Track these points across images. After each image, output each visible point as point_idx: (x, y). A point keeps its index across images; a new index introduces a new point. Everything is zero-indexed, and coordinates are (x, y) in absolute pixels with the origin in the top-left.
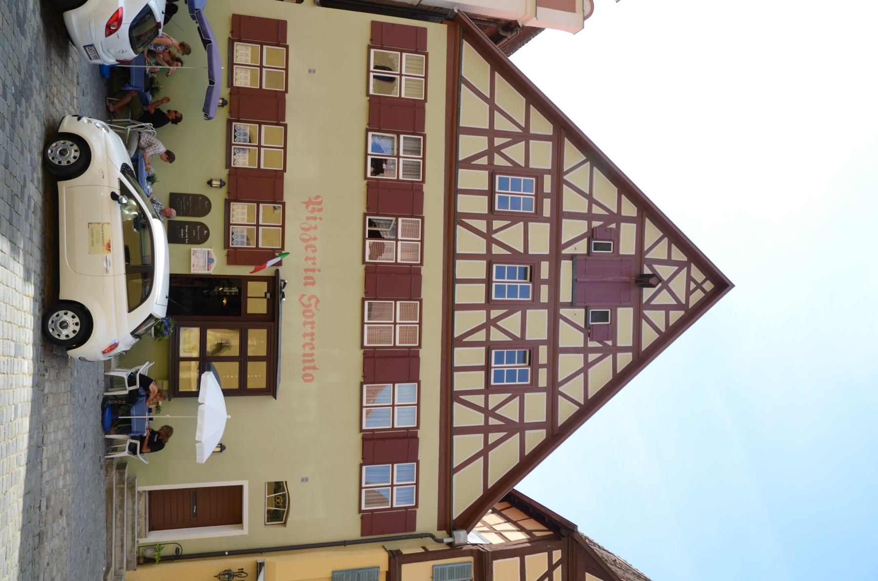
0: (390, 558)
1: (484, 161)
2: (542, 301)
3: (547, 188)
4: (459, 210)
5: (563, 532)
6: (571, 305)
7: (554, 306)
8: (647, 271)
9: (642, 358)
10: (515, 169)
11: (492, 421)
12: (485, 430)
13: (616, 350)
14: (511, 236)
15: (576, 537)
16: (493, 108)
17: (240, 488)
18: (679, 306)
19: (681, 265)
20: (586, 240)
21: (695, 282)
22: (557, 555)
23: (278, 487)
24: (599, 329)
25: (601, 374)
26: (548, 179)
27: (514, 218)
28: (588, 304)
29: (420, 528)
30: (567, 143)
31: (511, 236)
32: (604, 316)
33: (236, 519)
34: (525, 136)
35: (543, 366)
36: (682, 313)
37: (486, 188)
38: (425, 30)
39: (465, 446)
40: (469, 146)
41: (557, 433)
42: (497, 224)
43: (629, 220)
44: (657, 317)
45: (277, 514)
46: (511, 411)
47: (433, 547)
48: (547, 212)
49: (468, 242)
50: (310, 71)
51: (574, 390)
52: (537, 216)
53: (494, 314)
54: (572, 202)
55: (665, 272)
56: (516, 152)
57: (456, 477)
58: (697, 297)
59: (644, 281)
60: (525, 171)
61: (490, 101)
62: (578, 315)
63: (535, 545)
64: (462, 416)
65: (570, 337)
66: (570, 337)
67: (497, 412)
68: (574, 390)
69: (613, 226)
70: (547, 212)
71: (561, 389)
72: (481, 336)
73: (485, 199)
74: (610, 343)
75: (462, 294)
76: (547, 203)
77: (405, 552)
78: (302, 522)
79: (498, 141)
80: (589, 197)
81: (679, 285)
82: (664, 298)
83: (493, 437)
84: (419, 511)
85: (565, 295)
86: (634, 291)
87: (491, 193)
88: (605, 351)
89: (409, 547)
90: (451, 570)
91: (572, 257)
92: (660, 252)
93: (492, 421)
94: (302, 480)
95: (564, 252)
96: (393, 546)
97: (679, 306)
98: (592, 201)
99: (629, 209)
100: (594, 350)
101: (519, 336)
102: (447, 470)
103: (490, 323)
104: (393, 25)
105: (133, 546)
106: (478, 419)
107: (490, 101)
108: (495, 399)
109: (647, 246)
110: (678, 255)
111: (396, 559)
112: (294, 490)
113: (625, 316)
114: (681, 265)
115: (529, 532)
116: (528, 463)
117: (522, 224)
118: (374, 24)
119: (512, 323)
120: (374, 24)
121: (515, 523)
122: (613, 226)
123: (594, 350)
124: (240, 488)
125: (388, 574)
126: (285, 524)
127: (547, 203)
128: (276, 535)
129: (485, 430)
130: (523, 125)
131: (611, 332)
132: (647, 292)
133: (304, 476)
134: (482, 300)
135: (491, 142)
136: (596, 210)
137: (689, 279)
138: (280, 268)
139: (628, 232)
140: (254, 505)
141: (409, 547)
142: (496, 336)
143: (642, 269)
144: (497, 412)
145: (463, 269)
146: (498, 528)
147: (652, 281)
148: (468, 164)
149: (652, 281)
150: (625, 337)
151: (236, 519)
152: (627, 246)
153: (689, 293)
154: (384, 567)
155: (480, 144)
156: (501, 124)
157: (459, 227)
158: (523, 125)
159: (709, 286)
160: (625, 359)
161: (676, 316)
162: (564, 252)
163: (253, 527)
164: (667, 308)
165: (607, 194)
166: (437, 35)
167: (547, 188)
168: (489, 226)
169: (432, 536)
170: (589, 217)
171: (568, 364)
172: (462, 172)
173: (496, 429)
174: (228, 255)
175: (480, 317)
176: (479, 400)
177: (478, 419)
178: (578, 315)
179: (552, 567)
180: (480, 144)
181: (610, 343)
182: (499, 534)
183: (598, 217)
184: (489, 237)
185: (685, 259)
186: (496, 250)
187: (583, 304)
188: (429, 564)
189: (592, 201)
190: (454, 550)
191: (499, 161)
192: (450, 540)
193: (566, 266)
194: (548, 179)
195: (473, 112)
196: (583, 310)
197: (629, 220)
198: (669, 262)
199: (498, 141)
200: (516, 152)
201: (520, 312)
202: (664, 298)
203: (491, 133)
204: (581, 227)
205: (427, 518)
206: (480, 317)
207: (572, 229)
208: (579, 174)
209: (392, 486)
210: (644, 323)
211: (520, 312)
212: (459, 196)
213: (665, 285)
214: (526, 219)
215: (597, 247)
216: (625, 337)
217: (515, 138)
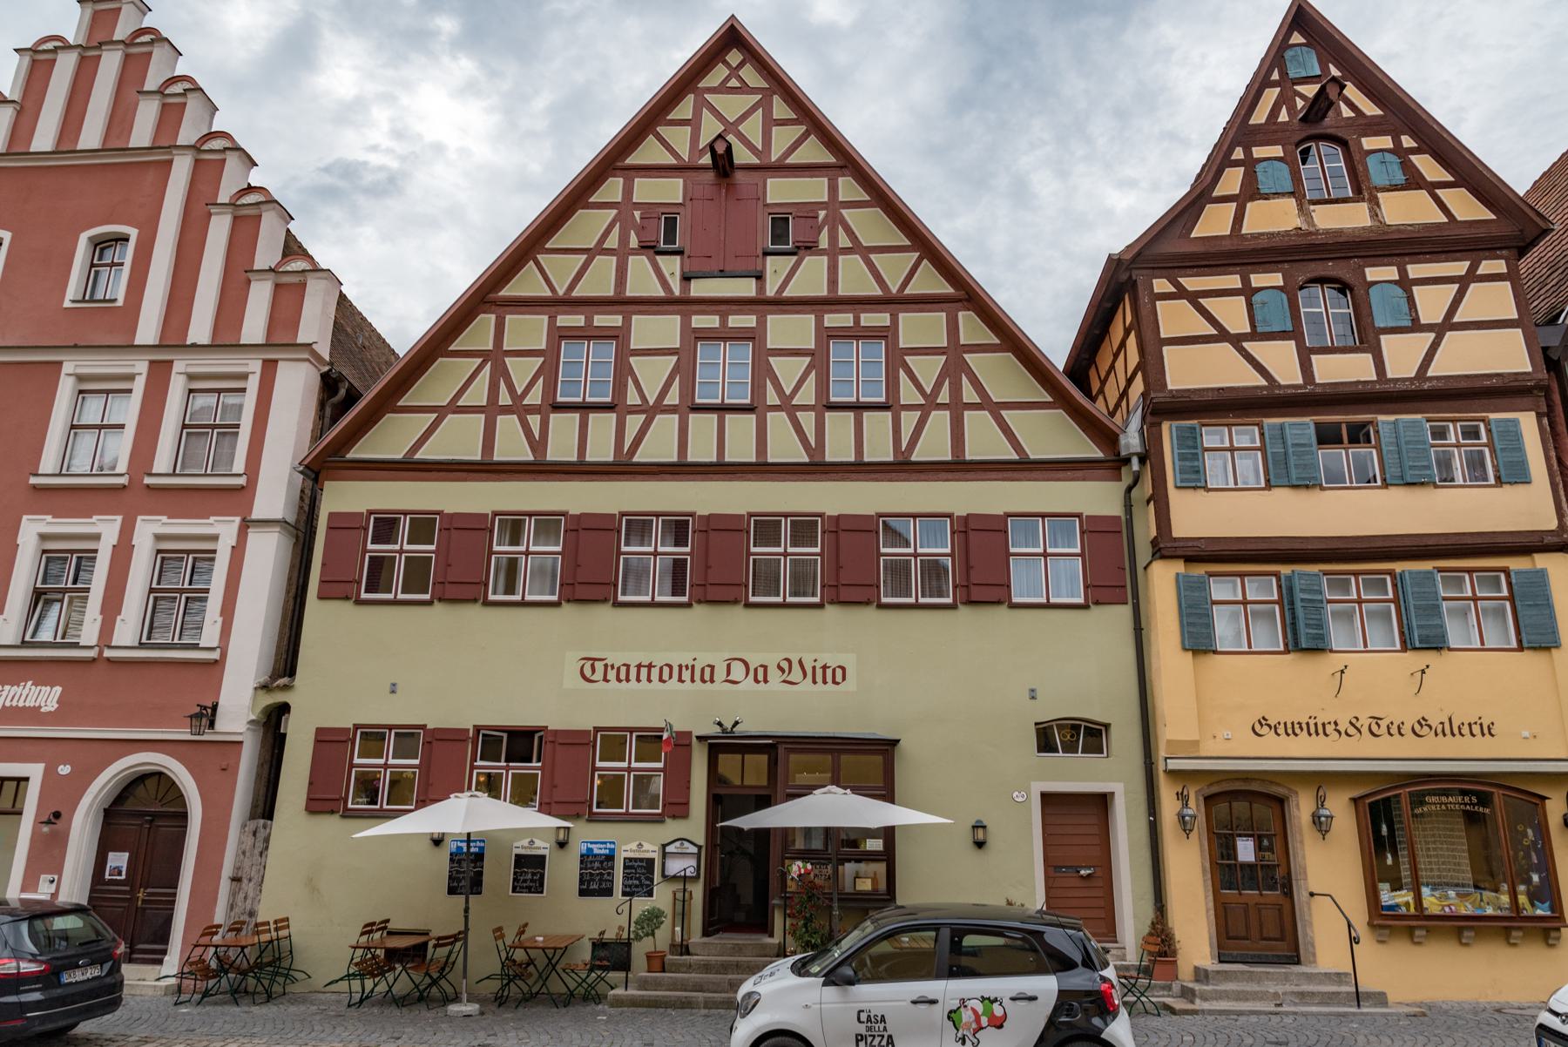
0: (1163, 557)
1: (534, 421)
2: (754, 325)
3: (578, 320)
4: (611, 459)
5: (1124, 277)
6: (760, 277)
7: (761, 304)
8: (706, 160)
9: (847, 161)
10: (549, 372)
11: (944, 397)
12: (957, 408)
13: (833, 204)
14: (652, 375)
15: (1128, 256)
16: (454, 408)
17: (1046, 797)
18: (765, 104)
19: (701, 104)
20: (659, 258)
21: (727, 79)
22: (1161, 285)
23: (1046, 739)
24: (790, 233)
25: (870, 226)
26: (564, 320)
27: (623, 372)
28: (760, 252)
29: (1114, 508)
30: (506, 292)
31: (652, 375)
32: (780, 225)
33: (1102, 802)
34: (496, 357)
35: (857, 320)
36: (776, 99)
37: (577, 416)
38: (332, 515)
39: (984, 440)
40: (512, 445)
41: (966, 295)
42: (633, 398)
43: (628, 191)
44: (782, 138)
45: (1086, 736)
46: (928, 369)
47: (1146, 487)
48: (615, 320)
49: (660, 445)
50: (393, 692)
51: (895, 269)
52: (619, 336)
53: (772, 398)
54: (600, 281)
55: (710, 128)
56: (522, 371)
57: (1033, 456)
58: (750, 75)
59: (723, 164)
60: (550, 358)
61: (441, 412)
62: (776, 268)
63: (1145, 327)
64: (934, 444)
65: (810, 277)
66: (810, 277)
67: (928, 391)
68: (895, 269)
69: (637, 214)
70: (615, 320)
71: (561, 292)
72: (807, 420)
73: (593, 417)
74: (822, 214)
75: (741, 449)
76: (601, 320)
77: (1154, 533)
78: (1107, 701)
79: (505, 399)
80: (591, 253)
81: (732, 106)
82: (753, 128)
83: (969, 394)
84: (1088, 511)
85: (747, 288)
86: (739, 177)
87: (585, 408)
88: (836, 221)
89: (1146, 528)
90: (1182, 458)
91: (686, 279)
92: (679, 138)
93: (944, 397)
94: (1033, 698)
95: (677, 292)
96: (1143, 551)
97: (765, 104)
98: (600, 250)
99: (613, 189)
100: (833, 238)
101: (808, 359)
102: (1023, 468)
103: (788, 406)
104: (323, 565)
105: (1226, 976)
106: (940, 421)
107: (441, 412)
108: (908, 394)
109: (672, 161)
110: (685, 109)
111: (1165, 548)
112: (1050, 711)
113: (780, 191)
114: (701, 104)
115: (1127, 333)
116: (1011, 341)
117: (632, 360)
118: (321, 597)
119: (788, 371)
120: (321, 597)
121: (1116, 356)
122: (637, 214)
123: (833, 238)
124: (1046, 797)
125: (1189, 560)
126: (1107, 726)
127: (601, 320)
128: (1124, 738)
129: (957, 408)
130: (479, 360)
131: (807, 211)
132: (742, 156)
133: (1027, 695)
134: (751, 419)
135: (506, 410)
136: (612, 242)
137: (723, 89)
138: (696, 733)
139: (649, 190)
140: (1076, 774)
141: (1146, 528)
142: (807, 395)
143: (704, 168)
144: (928, 391)
145: (702, 450)
146: (1122, 384)
147: (720, 148)
148: (538, 445)
149: (720, 148)
150: (813, 190)
151: (1102, 802)
152: (671, 190)
153: (744, 89)
154: (1179, 567)
155: (507, 426)
156: (478, 394)
157: (636, 459)
158: (479, 360)
159: (734, 57)
160: (848, 188)
161: (780, 109)
162: (677, 292)
163: (1111, 774)
164: (769, 123)
165: (588, 226)
166: (346, 497)
167: (578, 320)
168: (635, 410)
169: (1129, 489)
170: (622, 254)
171: (854, 279)
172: (551, 456)
173: (956, 390)
174: (674, 817)
175: (778, 423)
176: (909, 420)
177: (940, 421)
178: (776, 268)
179: (1181, 293)
180: (507, 426)
181: (822, 214)
182: (1130, 381)
183: (624, 239)
184: (651, 411)
185: (690, 98)
186: (673, 398)
187: (759, 260)
188: (1173, 494)
189: (600, 250)
190: (1150, 455)
191: (535, 397)
192: (1135, 461)
193: (699, 289)
194: (564, 320)
195: (459, 439)
196: (769, 258)
197: (628, 191)
198: (694, 123)
199: (505, 399)
200: (522, 371)
201: (771, 359)
202: (753, 128)
203: (491, 410)
204: (639, 266)
205: (1098, 498)
206: (778, 423)
207: (643, 279)
208: (556, 272)
209: (1045, 555)
210: (790, 161)
211: (771, 359)
212: (588, 459)
213: (732, 127)
214: (625, 354)
215: (670, 238)
216: (813, 190)
217: (500, 373)
